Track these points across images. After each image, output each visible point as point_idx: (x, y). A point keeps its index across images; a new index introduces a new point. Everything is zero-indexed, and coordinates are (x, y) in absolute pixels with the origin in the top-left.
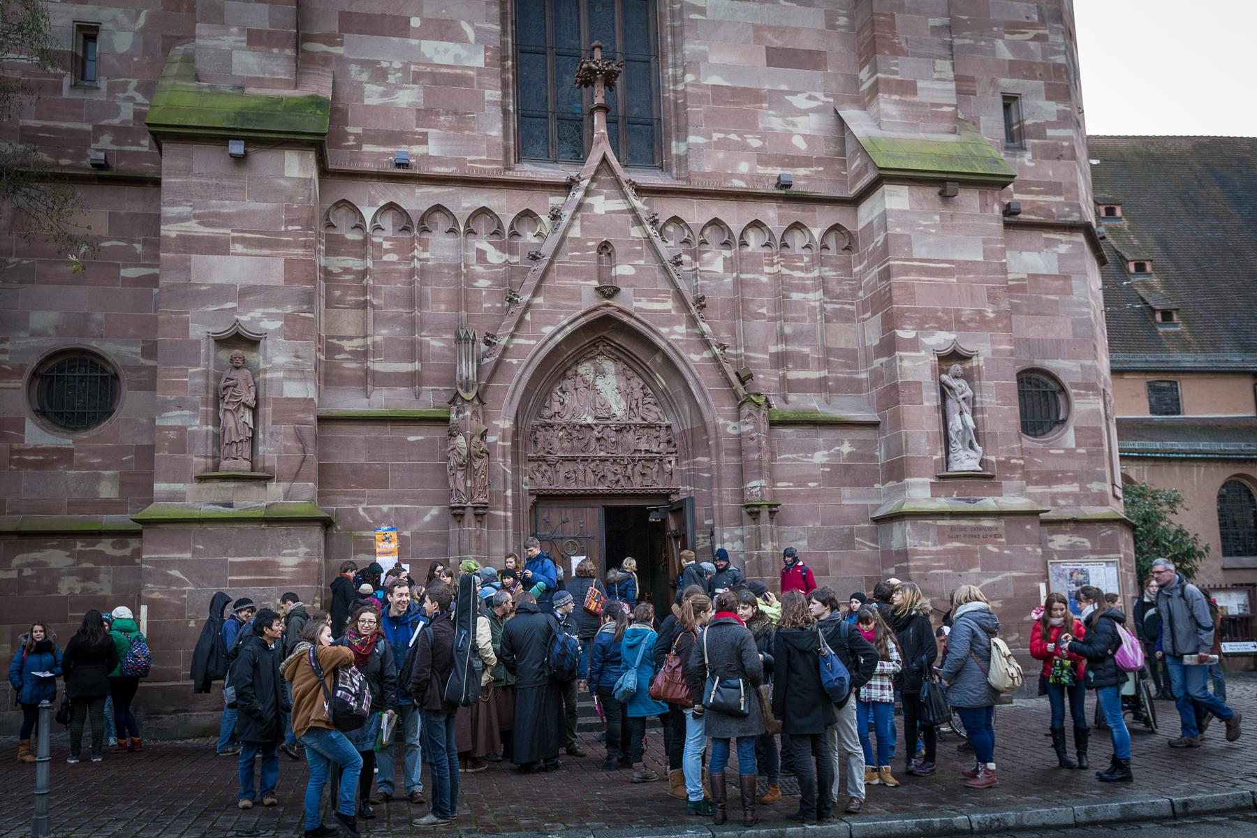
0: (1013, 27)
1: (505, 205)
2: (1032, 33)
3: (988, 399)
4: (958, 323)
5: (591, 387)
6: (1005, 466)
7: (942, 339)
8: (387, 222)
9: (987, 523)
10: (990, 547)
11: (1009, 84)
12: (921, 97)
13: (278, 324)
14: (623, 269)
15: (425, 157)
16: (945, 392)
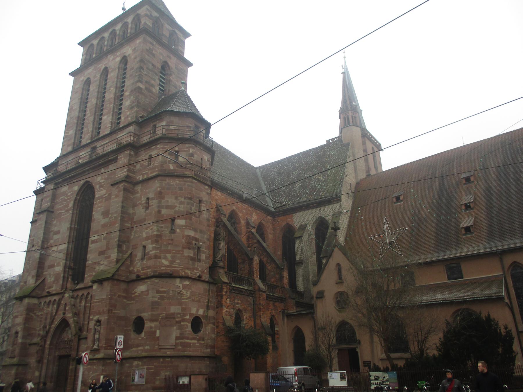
0: (147, 228)
1: (56, 298)
2: (150, 228)
3: (102, 331)
4: (99, 313)
5: (67, 332)
6: (102, 347)
7: (96, 317)
8: (46, 304)
9: (95, 361)
10: (95, 367)
11: (144, 243)
12: (111, 258)
13: (20, 329)
14: (67, 308)
15: (53, 290)
16: (95, 329)
